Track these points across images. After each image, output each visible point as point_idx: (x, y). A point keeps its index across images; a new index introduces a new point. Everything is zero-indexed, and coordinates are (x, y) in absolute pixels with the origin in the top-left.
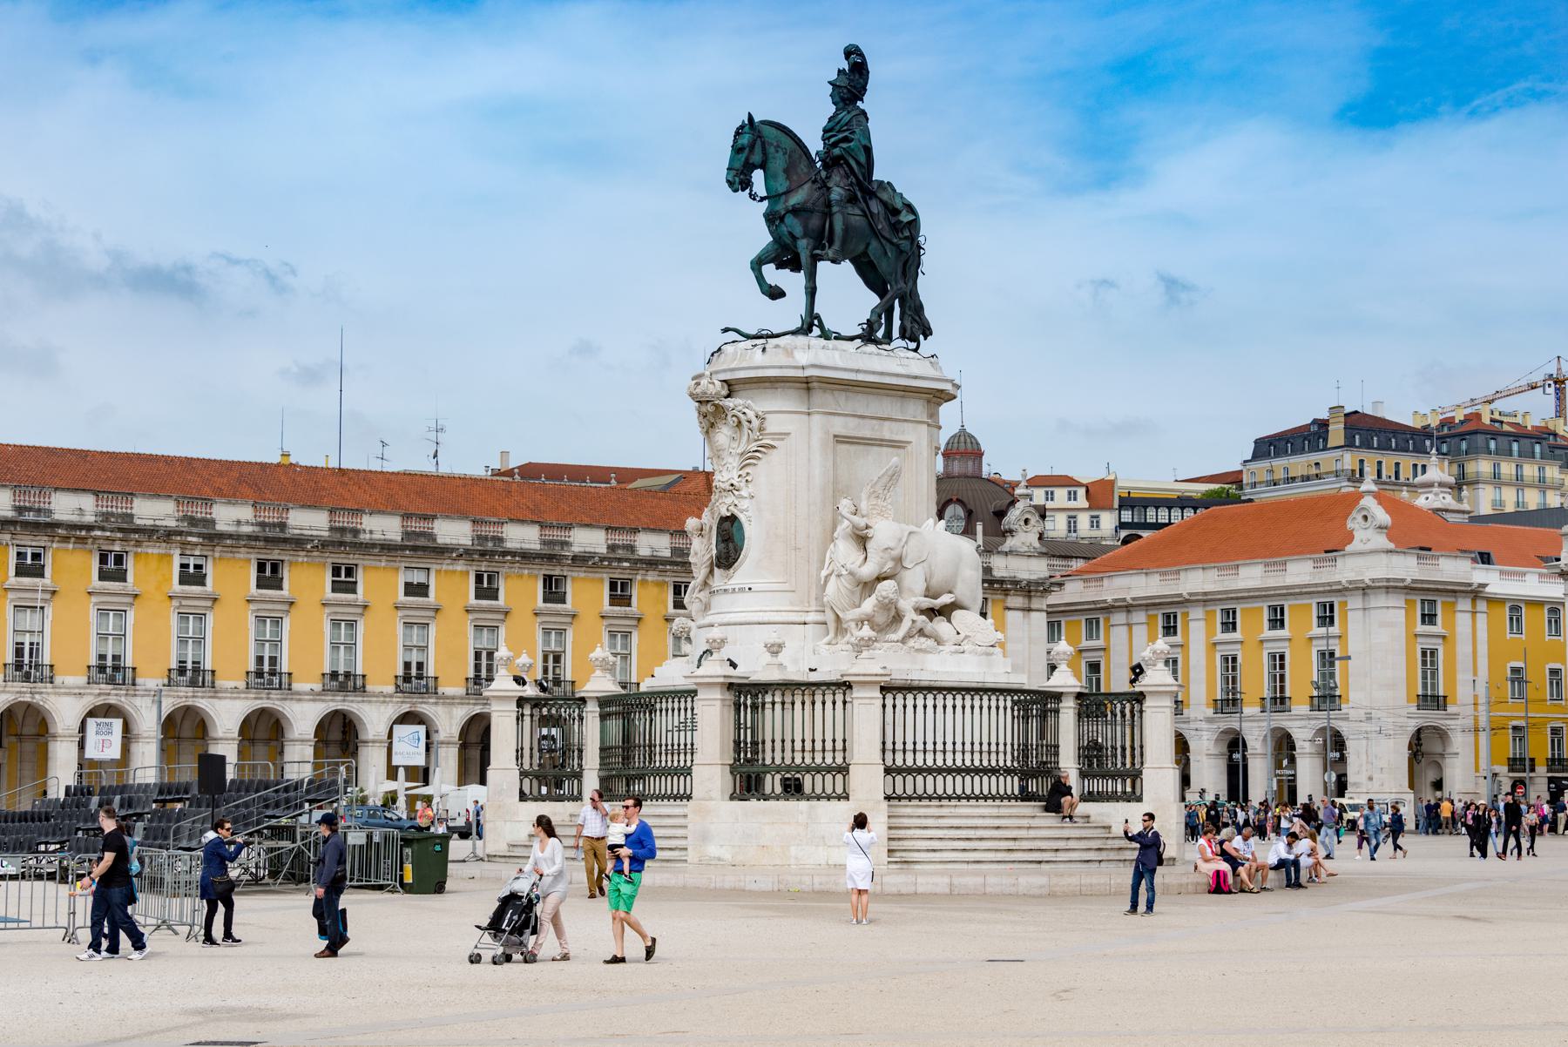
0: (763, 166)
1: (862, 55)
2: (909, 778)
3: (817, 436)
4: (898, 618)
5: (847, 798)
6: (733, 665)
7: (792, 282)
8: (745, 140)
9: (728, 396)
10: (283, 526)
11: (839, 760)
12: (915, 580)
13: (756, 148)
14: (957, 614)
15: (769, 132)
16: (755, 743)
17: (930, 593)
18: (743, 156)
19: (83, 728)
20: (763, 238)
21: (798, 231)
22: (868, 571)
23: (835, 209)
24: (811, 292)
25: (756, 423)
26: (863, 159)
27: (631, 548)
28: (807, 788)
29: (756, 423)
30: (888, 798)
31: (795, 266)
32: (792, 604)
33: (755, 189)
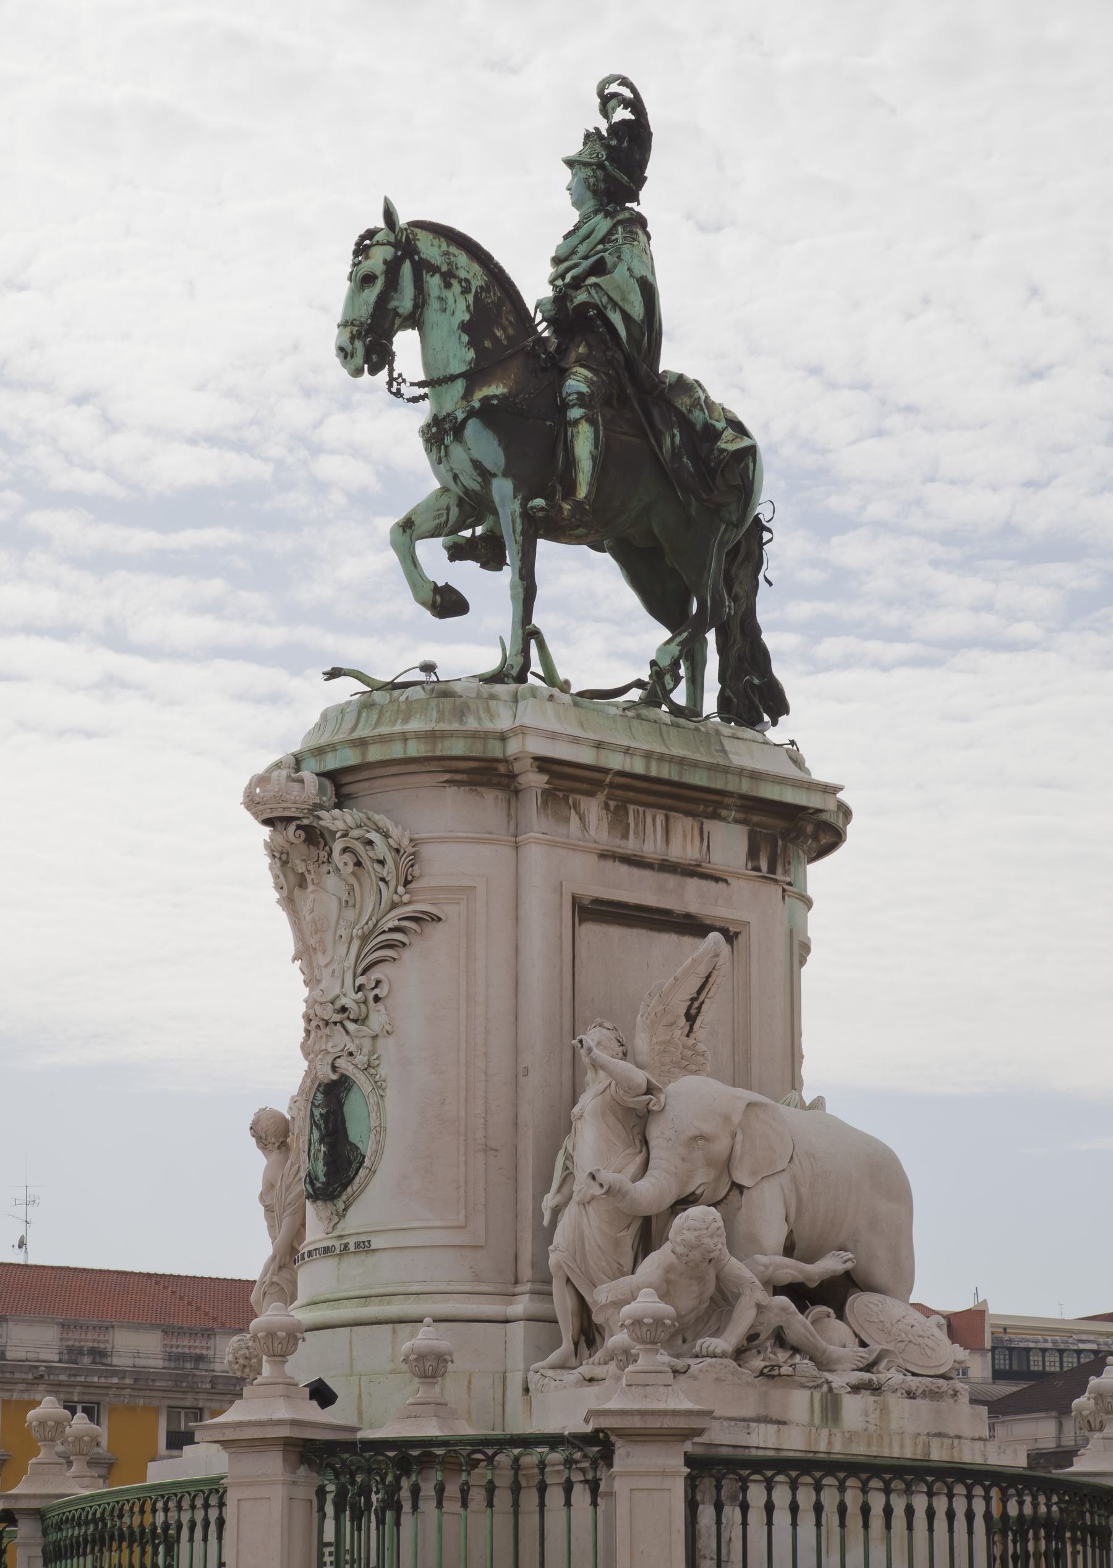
0: (414, 320)
6: (322, 1394)
7: (488, 589)
9: (339, 805)
12: (768, 1216)
15: (430, 249)
18: (372, 294)
20: (420, 479)
22: (651, 1191)
23: (575, 413)
26: (637, 310)
31: (488, 553)
32: (478, 1278)
33: (399, 366)
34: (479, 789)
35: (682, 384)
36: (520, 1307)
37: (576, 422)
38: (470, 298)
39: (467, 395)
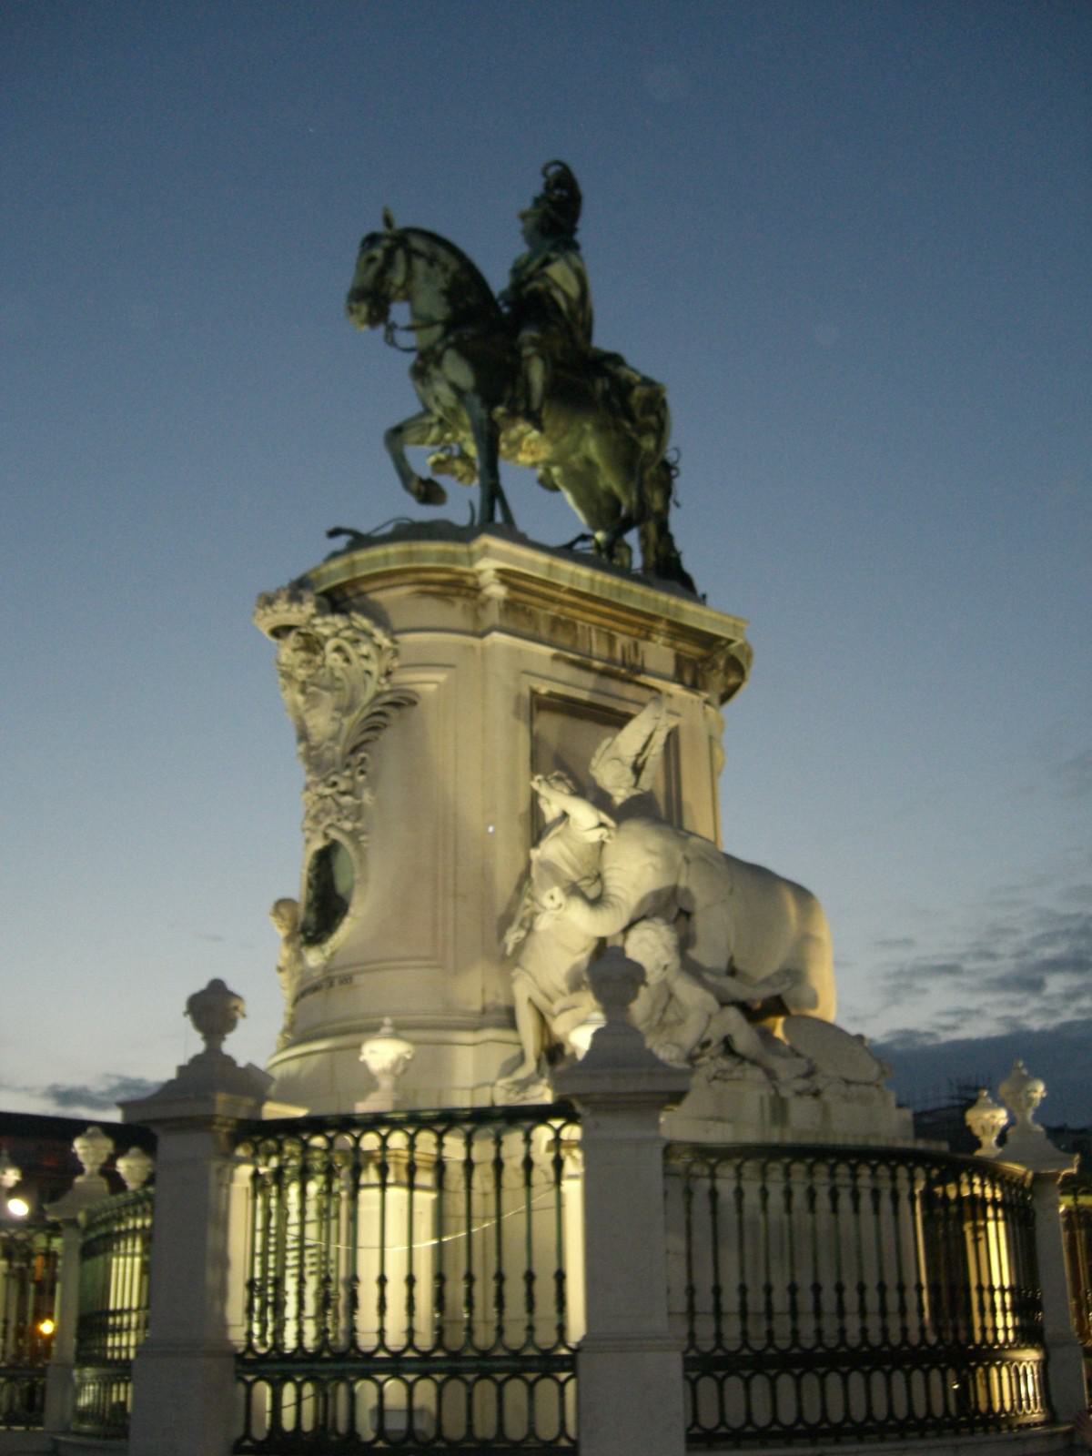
15: (417, 243)
18: (373, 269)
34: (450, 598)
37: (529, 358)
38: (448, 276)
39: (446, 334)
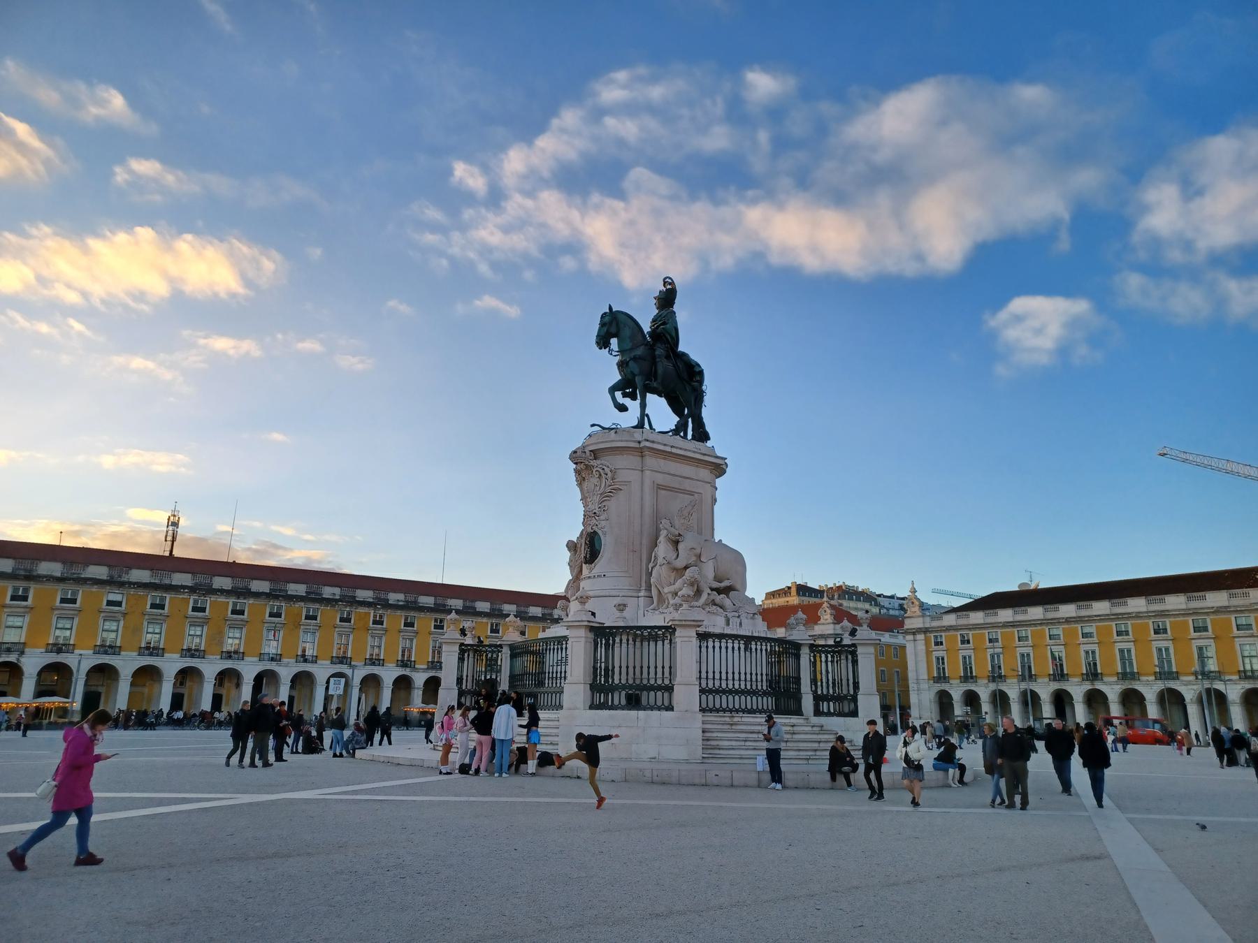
1: (672, 283)
2: (717, 697)
3: (647, 483)
4: (698, 593)
5: (672, 709)
6: (593, 614)
7: (634, 406)
8: (607, 319)
10: (416, 602)
11: (666, 682)
13: (614, 326)
14: (732, 593)
15: (621, 318)
16: (607, 669)
17: (718, 579)
19: (328, 682)
21: (636, 371)
22: (680, 563)
24: (643, 406)
25: (610, 474)
27: (551, 615)
28: (644, 702)
29: (610, 474)
30: (702, 710)
35: (684, 354)
36: (642, 594)
